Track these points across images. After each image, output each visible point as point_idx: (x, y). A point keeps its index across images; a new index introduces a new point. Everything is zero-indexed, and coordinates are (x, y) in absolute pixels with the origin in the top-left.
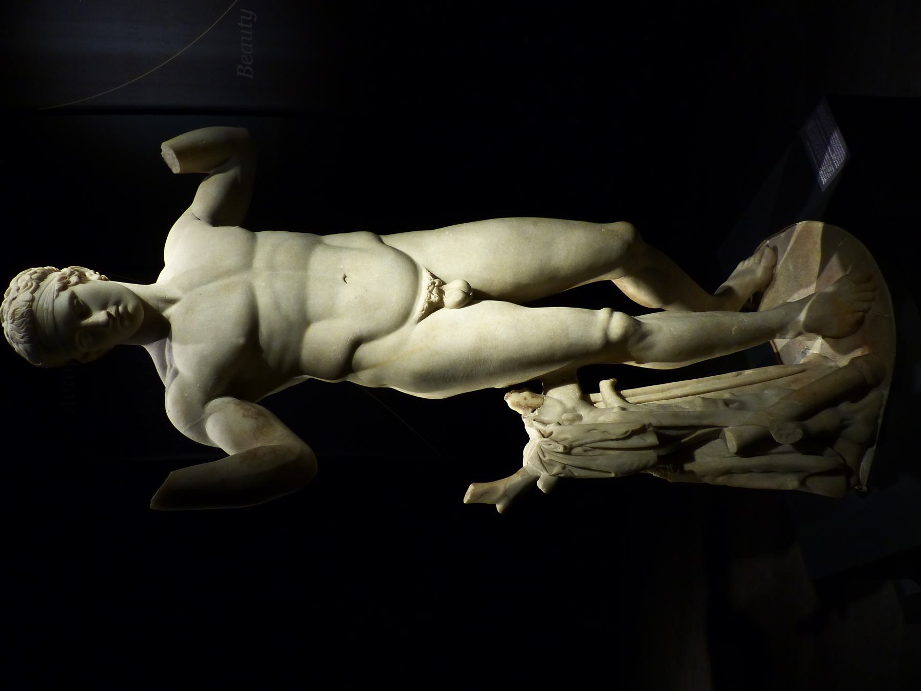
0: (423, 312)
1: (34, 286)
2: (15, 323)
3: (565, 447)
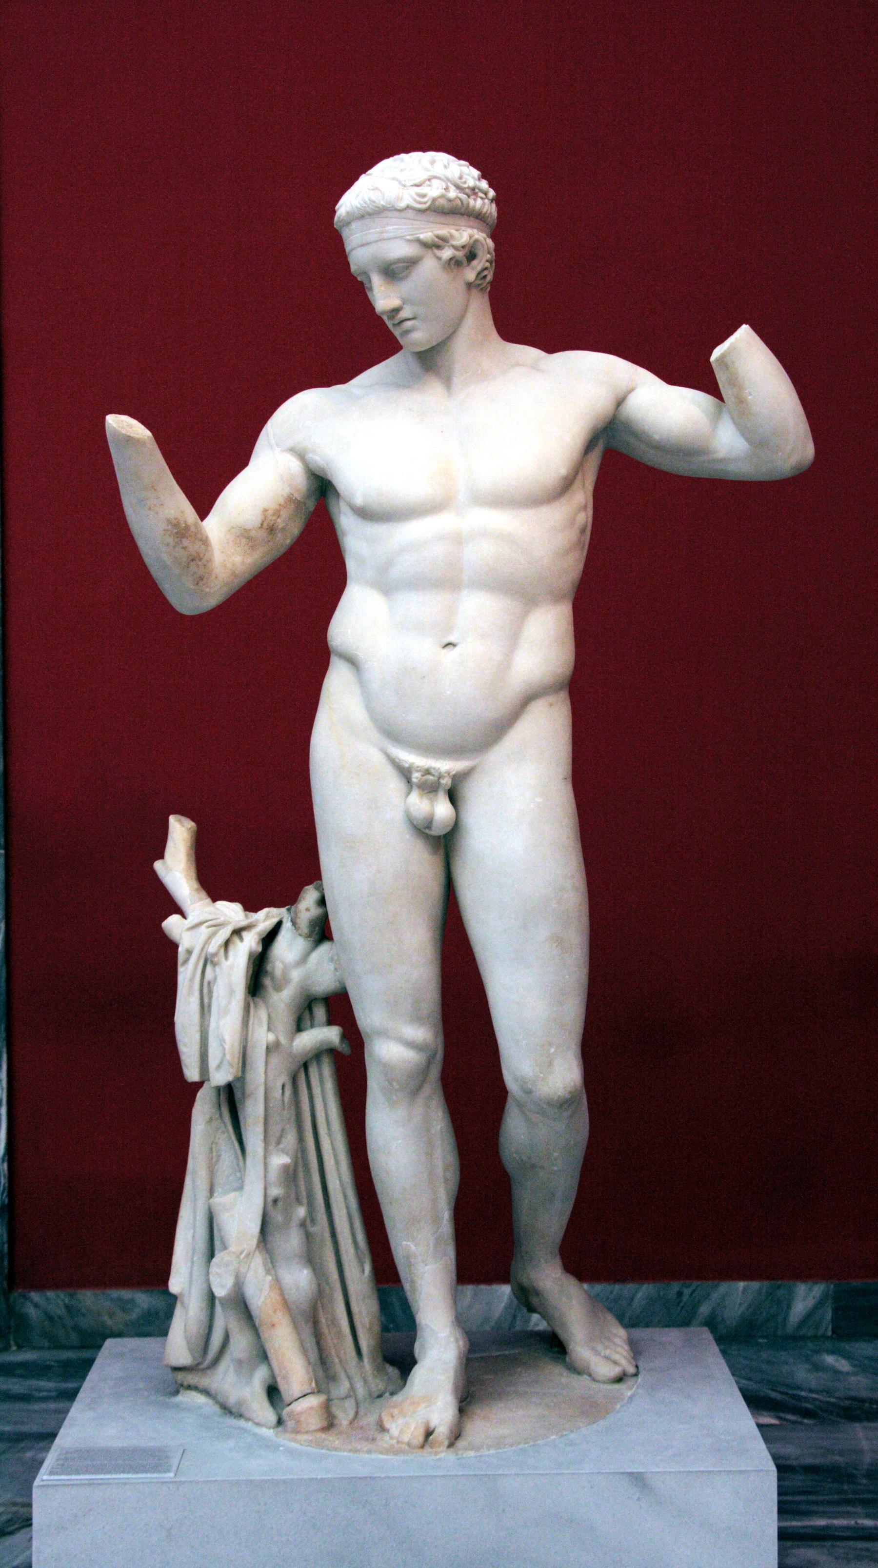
0: (397, 760)
1: (424, 206)
3: (215, 954)
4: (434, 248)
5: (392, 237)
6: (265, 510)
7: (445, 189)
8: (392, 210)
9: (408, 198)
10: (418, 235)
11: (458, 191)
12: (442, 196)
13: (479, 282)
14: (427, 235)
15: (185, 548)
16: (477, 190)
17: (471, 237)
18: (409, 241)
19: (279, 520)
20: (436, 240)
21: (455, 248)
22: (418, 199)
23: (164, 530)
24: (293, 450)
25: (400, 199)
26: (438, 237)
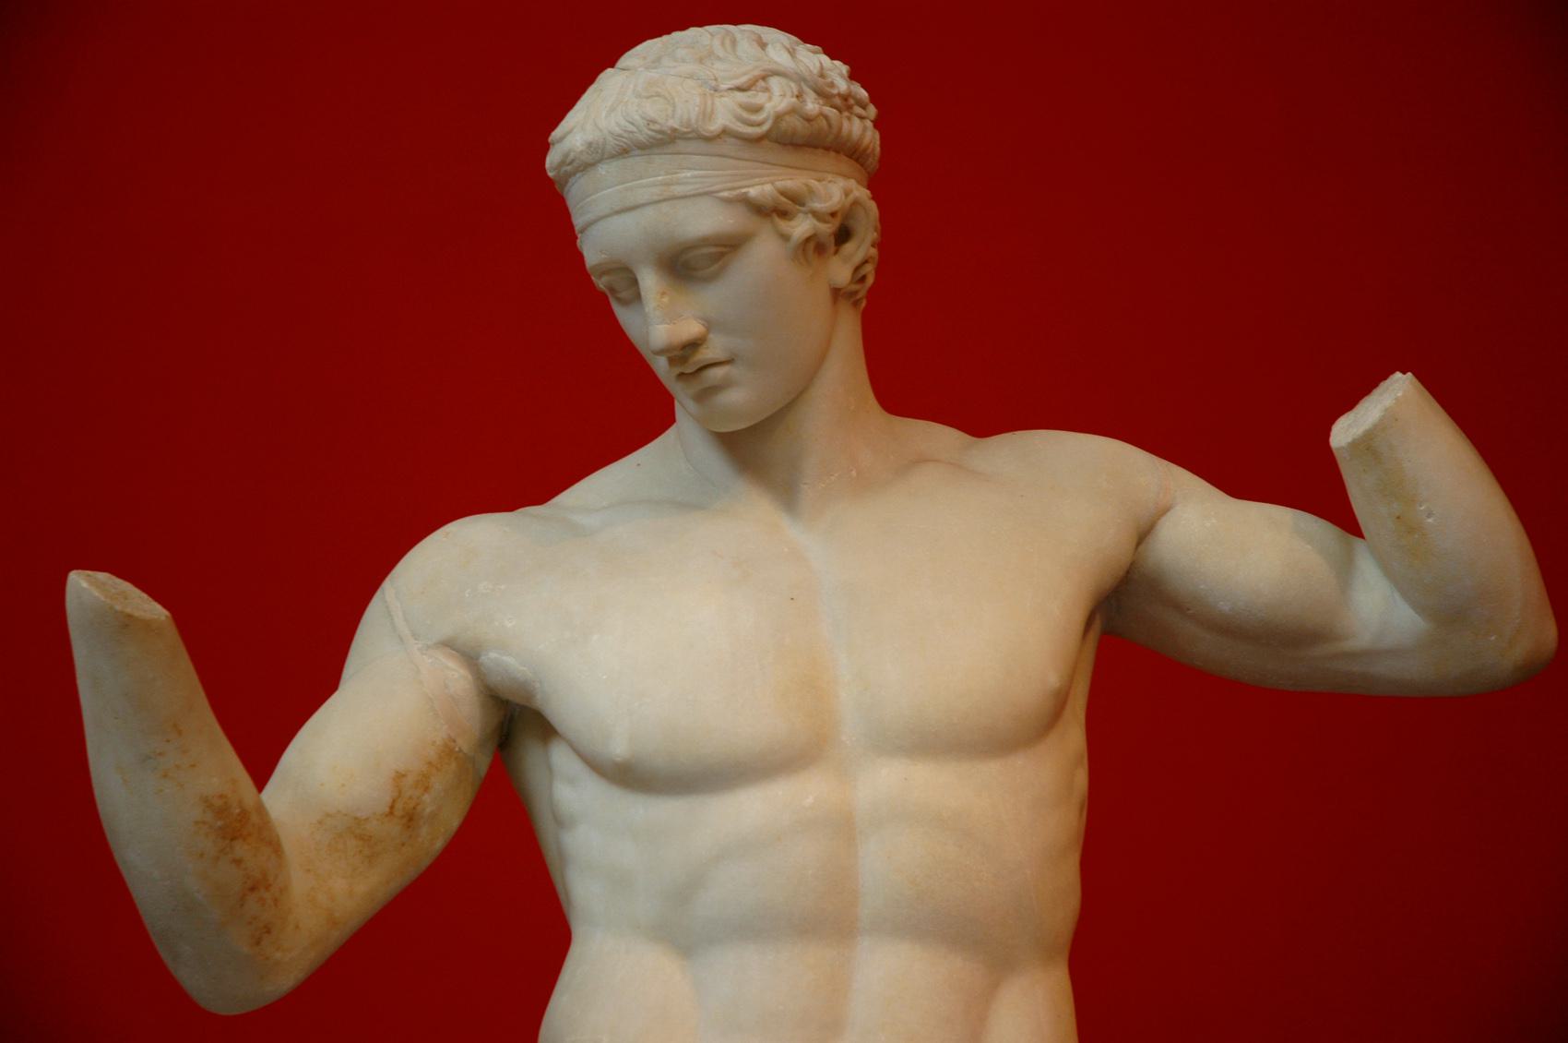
4: (775, 216)
5: (692, 193)
6: (400, 776)
7: (797, 97)
9: (725, 113)
10: (744, 190)
11: (821, 102)
12: (793, 111)
13: (855, 287)
14: (761, 190)
15: (238, 862)
16: (852, 101)
17: (847, 194)
18: (728, 201)
19: (426, 798)
20: (784, 199)
21: (815, 214)
22: (745, 115)
23: (196, 823)
24: (449, 645)
25: (707, 115)
26: (783, 193)
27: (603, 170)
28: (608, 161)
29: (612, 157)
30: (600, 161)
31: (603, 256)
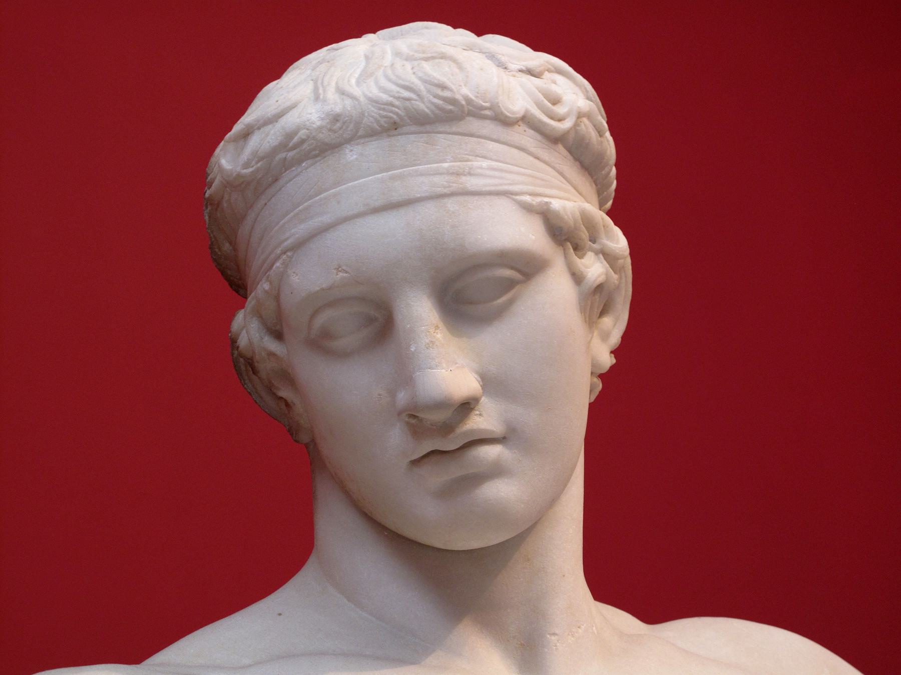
2: (399, 63)
5: (488, 189)
8: (485, 117)
10: (546, 200)
27: (351, 154)
28: (362, 141)
29: (373, 134)
30: (348, 141)
31: (341, 274)
